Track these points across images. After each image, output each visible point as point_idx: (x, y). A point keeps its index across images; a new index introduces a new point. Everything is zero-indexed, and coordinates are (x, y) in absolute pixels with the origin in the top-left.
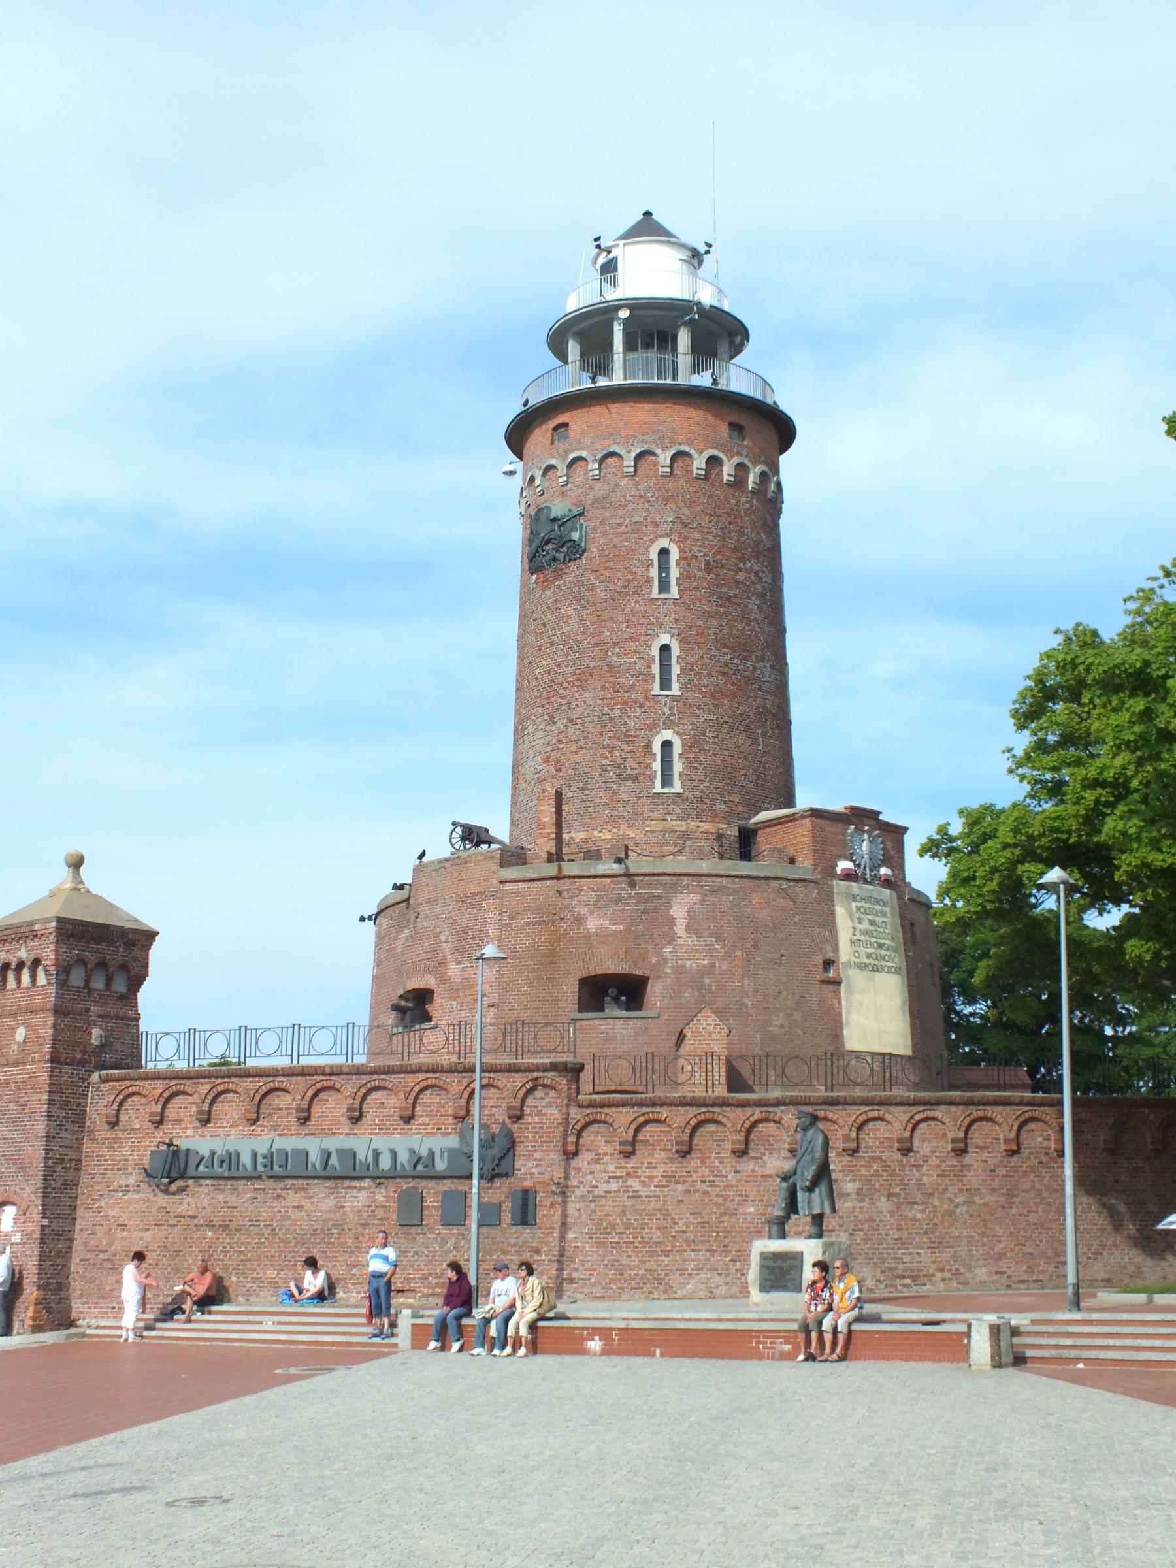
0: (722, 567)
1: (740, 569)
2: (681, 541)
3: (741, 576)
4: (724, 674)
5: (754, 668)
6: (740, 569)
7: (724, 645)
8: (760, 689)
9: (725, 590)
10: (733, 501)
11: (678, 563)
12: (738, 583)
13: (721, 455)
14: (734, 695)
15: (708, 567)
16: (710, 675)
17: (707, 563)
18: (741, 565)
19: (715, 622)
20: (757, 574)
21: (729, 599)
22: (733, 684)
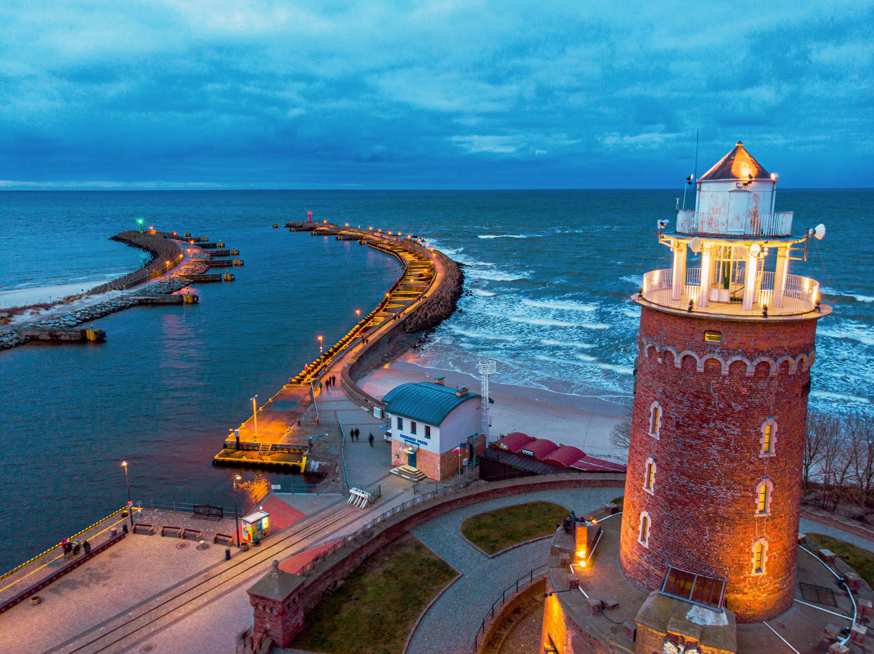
0: (689, 426)
1: (703, 428)
2: (665, 406)
3: (704, 432)
4: (680, 491)
5: (708, 489)
6: (703, 428)
7: (683, 474)
8: (712, 502)
9: (688, 441)
10: (704, 384)
11: (661, 419)
12: (699, 437)
13: (694, 354)
14: (686, 504)
15: (678, 426)
16: (671, 490)
17: (677, 422)
18: (705, 425)
19: (678, 460)
20: (720, 430)
21: (691, 446)
22: (687, 498)
